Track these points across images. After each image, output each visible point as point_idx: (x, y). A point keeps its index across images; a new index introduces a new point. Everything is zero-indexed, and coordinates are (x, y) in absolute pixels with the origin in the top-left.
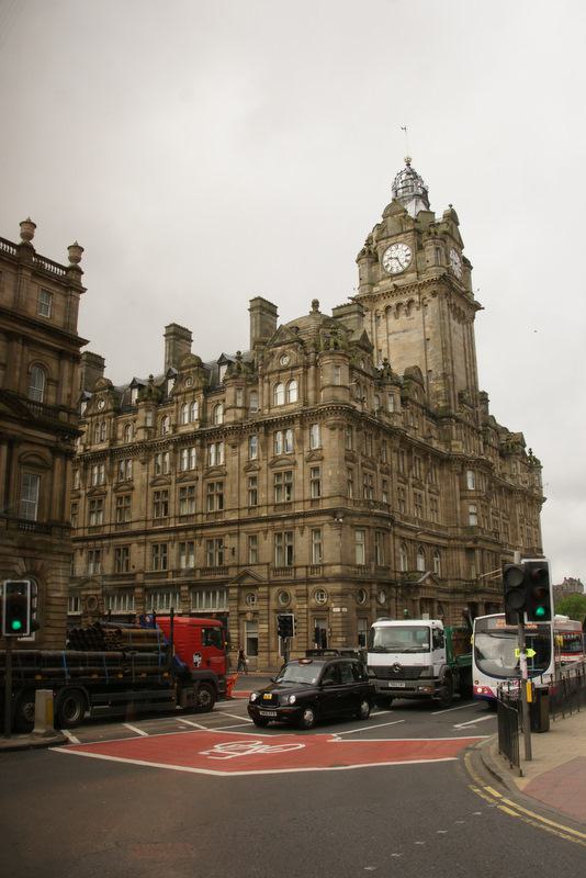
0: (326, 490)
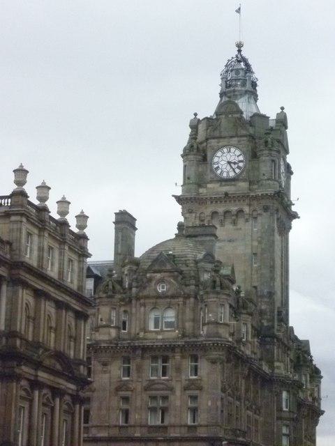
0: (203, 418)
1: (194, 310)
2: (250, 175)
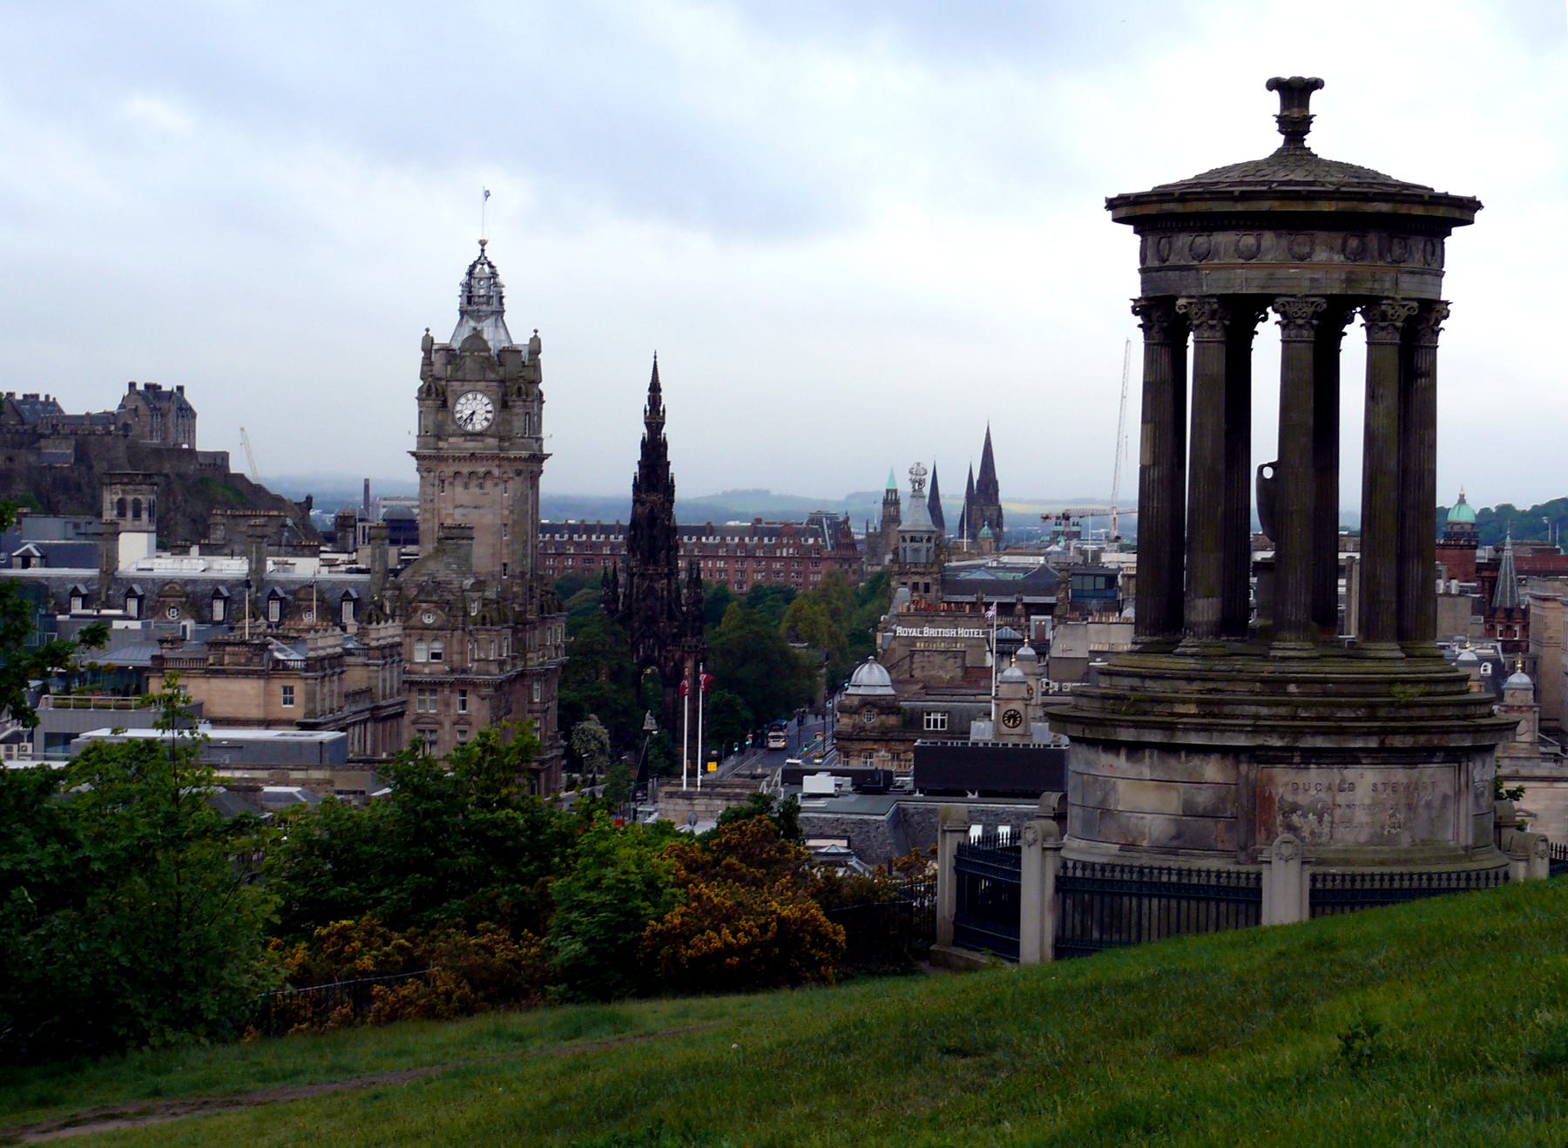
1: (461, 642)
2: (500, 431)
